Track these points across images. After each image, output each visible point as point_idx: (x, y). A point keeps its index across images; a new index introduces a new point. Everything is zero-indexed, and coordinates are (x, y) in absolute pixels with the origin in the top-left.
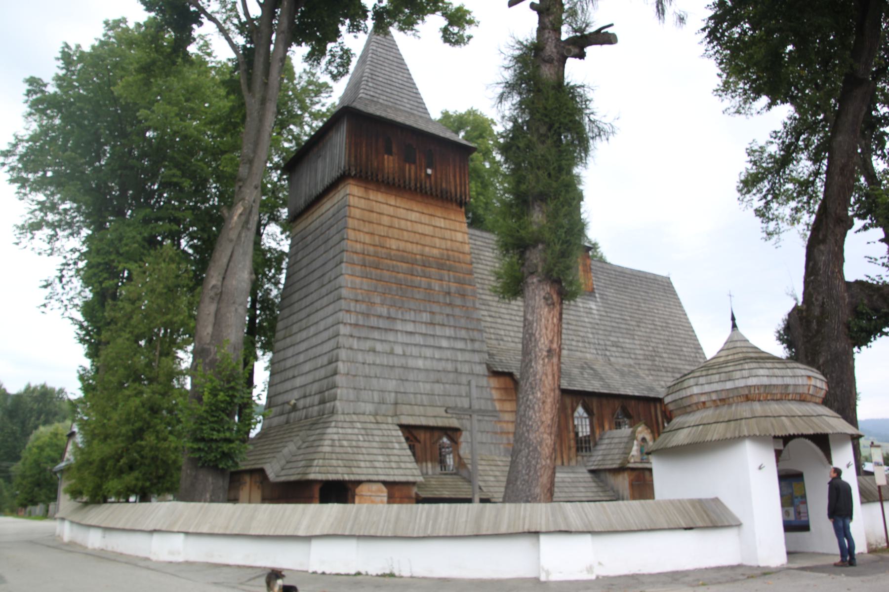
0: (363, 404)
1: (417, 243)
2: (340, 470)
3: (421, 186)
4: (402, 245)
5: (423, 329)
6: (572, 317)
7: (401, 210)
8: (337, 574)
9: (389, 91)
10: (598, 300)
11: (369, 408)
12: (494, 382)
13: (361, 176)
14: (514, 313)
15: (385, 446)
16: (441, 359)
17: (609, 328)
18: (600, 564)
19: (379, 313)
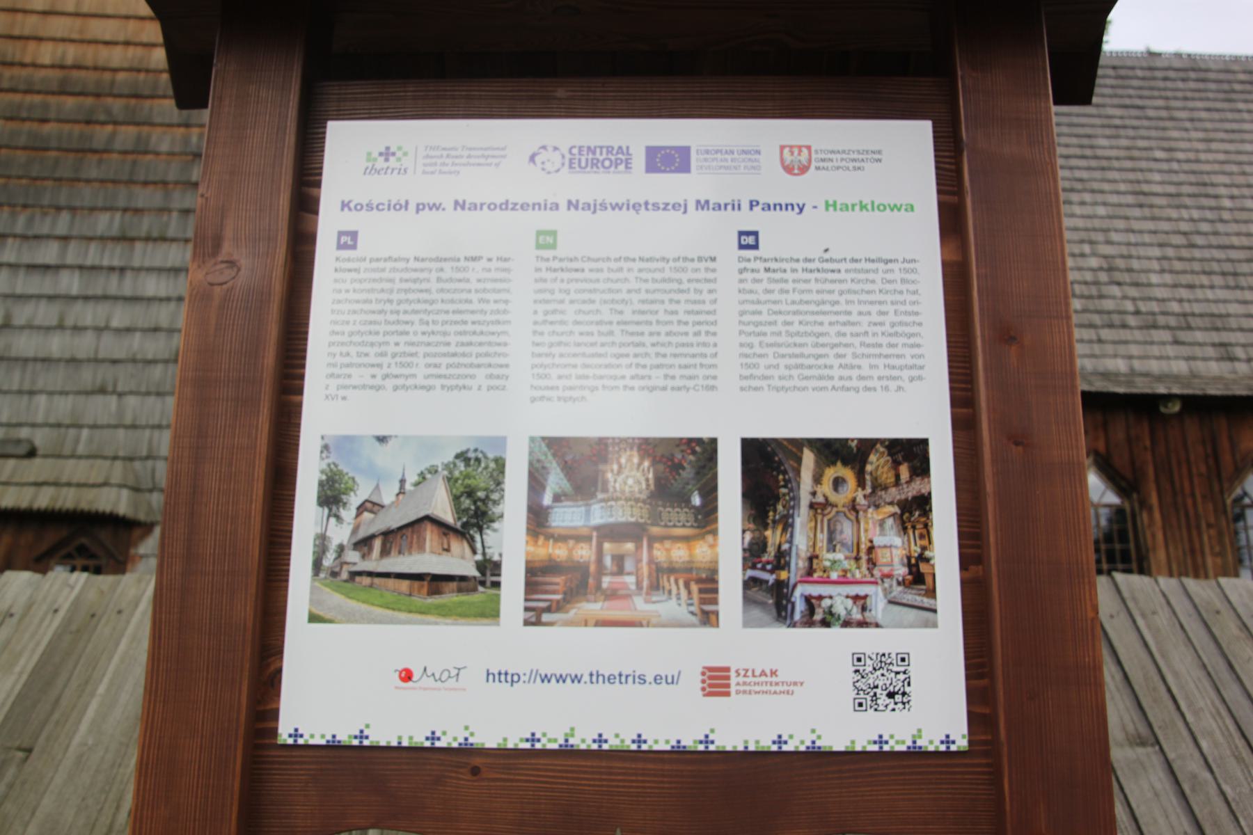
16: (129, 330)
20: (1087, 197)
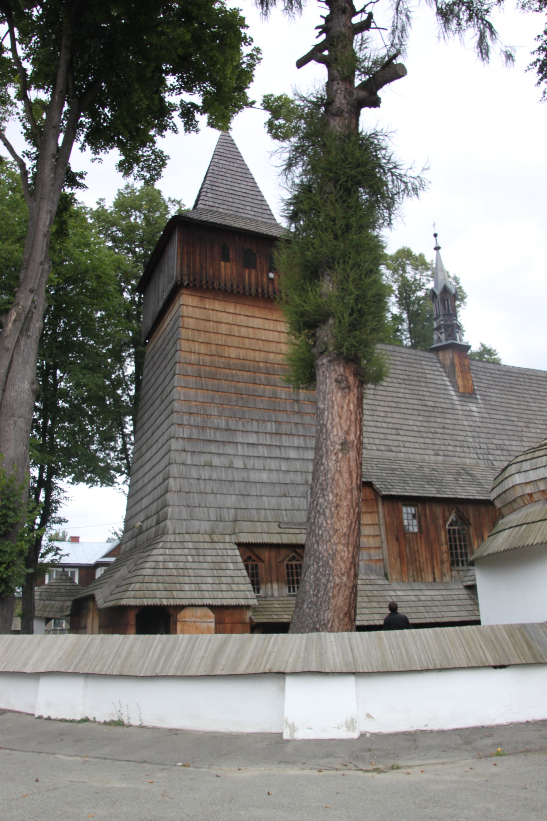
0: (197, 523)
1: (260, 351)
2: (158, 594)
3: (263, 291)
4: (242, 353)
5: (268, 440)
6: (448, 421)
7: (242, 317)
8: (62, 720)
9: (231, 200)
10: (480, 401)
11: (205, 526)
13: (194, 286)
14: (380, 419)
15: (218, 566)
17: (491, 431)
18: (369, 716)
19: (216, 425)
20: (534, 425)
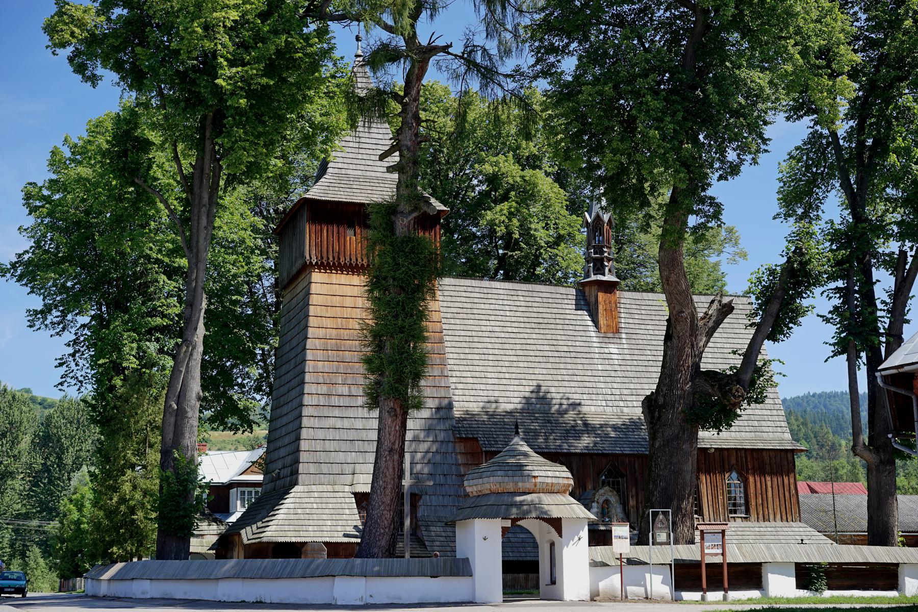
12: (460, 448)
